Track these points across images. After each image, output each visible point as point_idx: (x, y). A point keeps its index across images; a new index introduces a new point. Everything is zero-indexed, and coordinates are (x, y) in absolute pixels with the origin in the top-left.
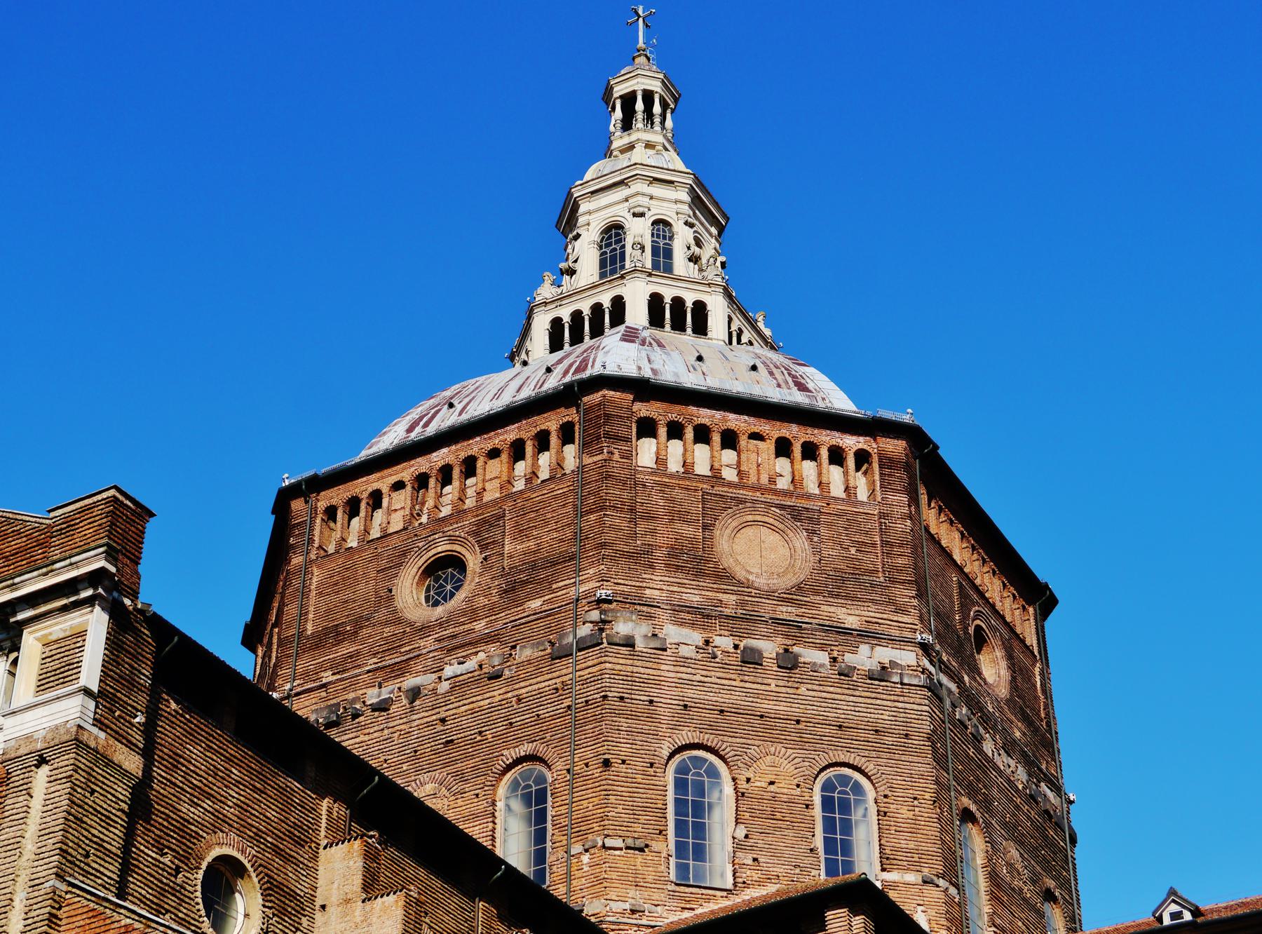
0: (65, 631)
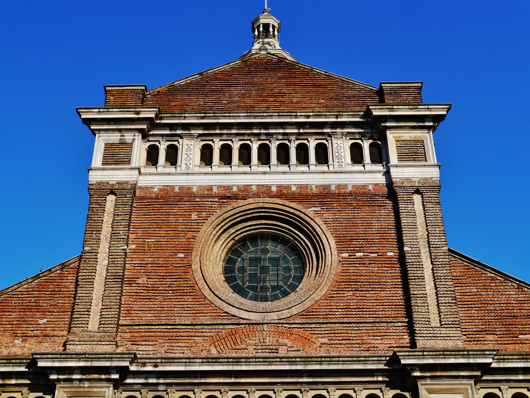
0: (411, 137)
